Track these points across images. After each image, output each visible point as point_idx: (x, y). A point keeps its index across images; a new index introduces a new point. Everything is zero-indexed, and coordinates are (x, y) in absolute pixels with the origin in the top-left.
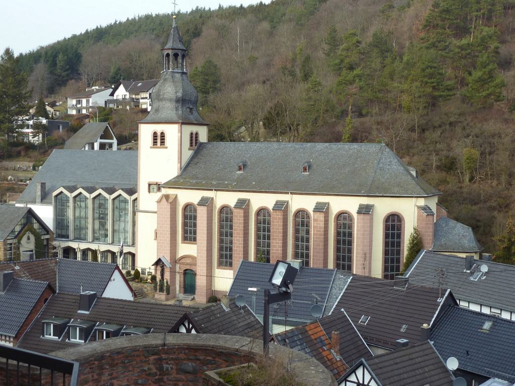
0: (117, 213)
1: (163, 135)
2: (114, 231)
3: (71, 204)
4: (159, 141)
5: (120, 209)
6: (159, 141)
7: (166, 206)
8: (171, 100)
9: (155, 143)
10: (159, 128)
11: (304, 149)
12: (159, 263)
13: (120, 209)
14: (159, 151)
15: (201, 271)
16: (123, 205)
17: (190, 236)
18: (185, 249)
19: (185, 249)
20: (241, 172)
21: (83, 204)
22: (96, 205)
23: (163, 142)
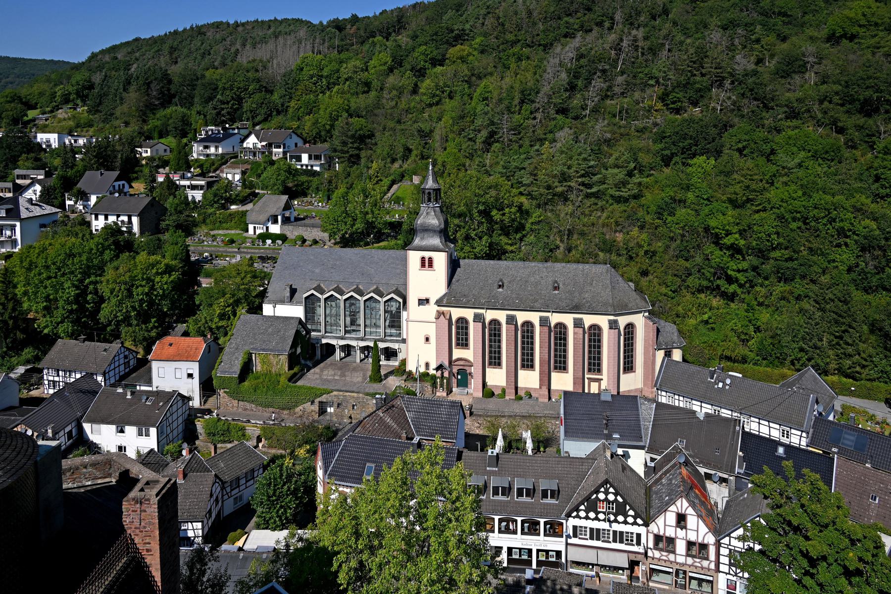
0: (367, 311)
1: (431, 260)
2: (365, 326)
3: (322, 301)
4: (427, 264)
5: (372, 309)
6: (427, 264)
7: (444, 322)
8: (435, 231)
9: (423, 265)
10: (427, 254)
11: (546, 268)
12: (440, 367)
13: (372, 309)
14: (427, 273)
15: (476, 371)
16: (374, 305)
17: (463, 343)
18: (457, 353)
19: (457, 353)
20: (500, 290)
21: (333, 304)
22: (347, 305)
23: (431, 265)
